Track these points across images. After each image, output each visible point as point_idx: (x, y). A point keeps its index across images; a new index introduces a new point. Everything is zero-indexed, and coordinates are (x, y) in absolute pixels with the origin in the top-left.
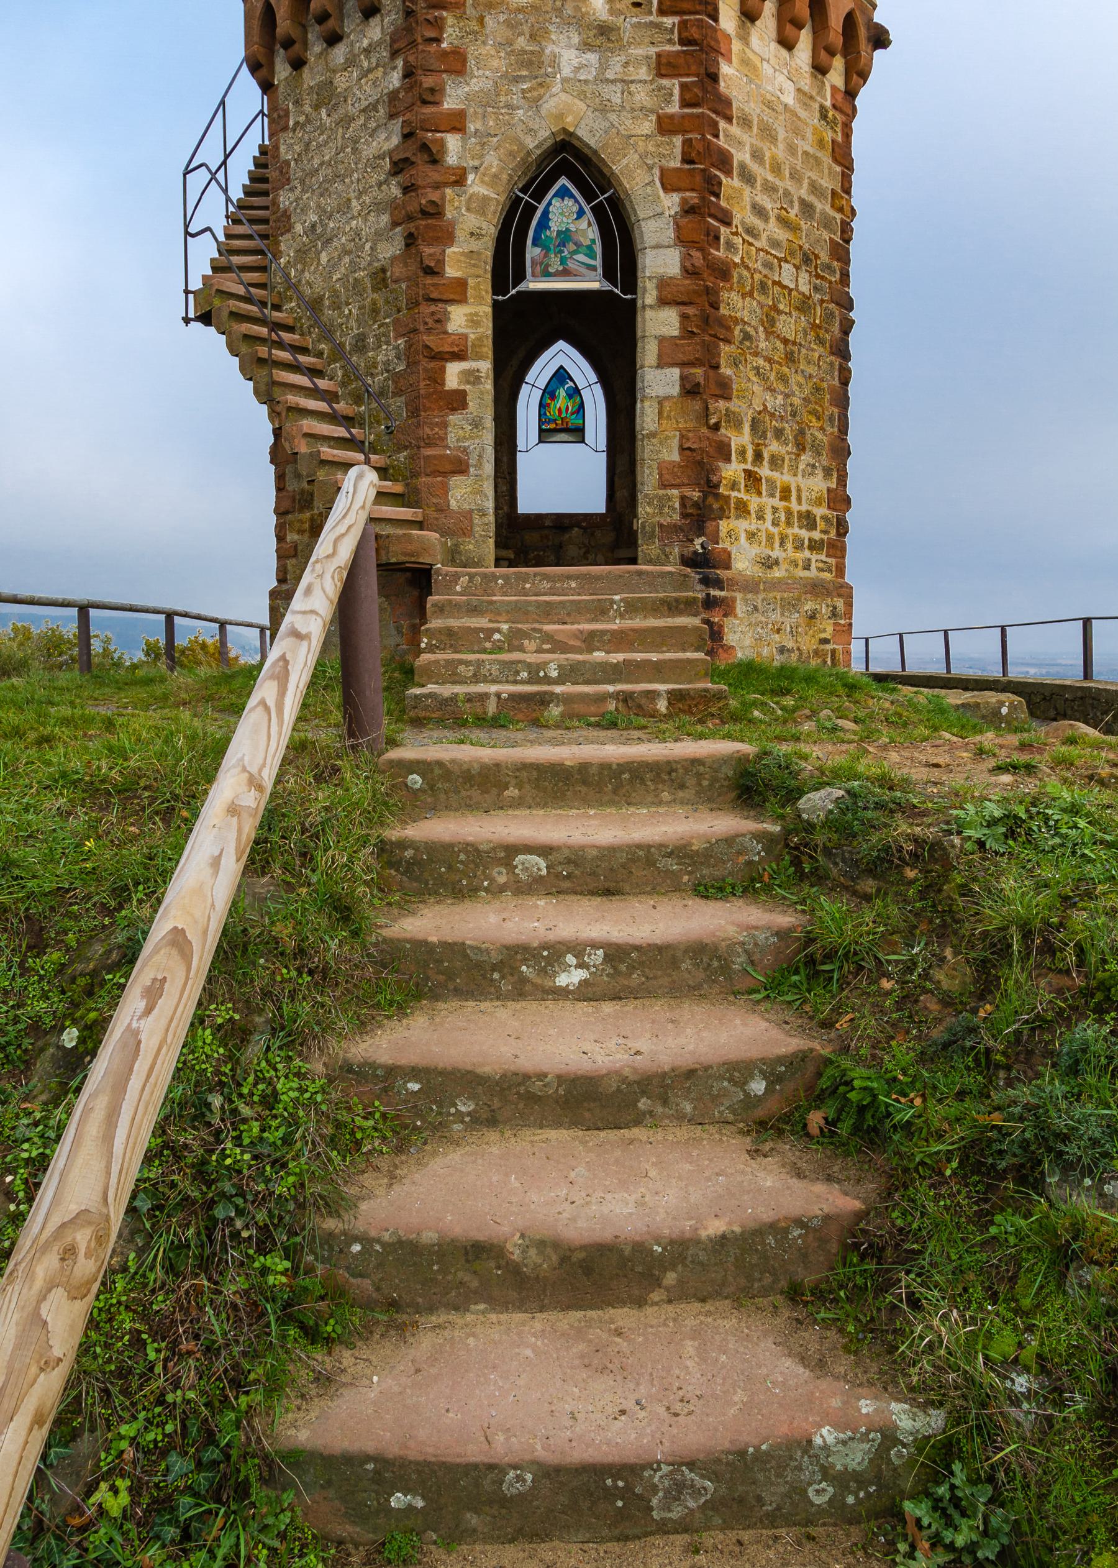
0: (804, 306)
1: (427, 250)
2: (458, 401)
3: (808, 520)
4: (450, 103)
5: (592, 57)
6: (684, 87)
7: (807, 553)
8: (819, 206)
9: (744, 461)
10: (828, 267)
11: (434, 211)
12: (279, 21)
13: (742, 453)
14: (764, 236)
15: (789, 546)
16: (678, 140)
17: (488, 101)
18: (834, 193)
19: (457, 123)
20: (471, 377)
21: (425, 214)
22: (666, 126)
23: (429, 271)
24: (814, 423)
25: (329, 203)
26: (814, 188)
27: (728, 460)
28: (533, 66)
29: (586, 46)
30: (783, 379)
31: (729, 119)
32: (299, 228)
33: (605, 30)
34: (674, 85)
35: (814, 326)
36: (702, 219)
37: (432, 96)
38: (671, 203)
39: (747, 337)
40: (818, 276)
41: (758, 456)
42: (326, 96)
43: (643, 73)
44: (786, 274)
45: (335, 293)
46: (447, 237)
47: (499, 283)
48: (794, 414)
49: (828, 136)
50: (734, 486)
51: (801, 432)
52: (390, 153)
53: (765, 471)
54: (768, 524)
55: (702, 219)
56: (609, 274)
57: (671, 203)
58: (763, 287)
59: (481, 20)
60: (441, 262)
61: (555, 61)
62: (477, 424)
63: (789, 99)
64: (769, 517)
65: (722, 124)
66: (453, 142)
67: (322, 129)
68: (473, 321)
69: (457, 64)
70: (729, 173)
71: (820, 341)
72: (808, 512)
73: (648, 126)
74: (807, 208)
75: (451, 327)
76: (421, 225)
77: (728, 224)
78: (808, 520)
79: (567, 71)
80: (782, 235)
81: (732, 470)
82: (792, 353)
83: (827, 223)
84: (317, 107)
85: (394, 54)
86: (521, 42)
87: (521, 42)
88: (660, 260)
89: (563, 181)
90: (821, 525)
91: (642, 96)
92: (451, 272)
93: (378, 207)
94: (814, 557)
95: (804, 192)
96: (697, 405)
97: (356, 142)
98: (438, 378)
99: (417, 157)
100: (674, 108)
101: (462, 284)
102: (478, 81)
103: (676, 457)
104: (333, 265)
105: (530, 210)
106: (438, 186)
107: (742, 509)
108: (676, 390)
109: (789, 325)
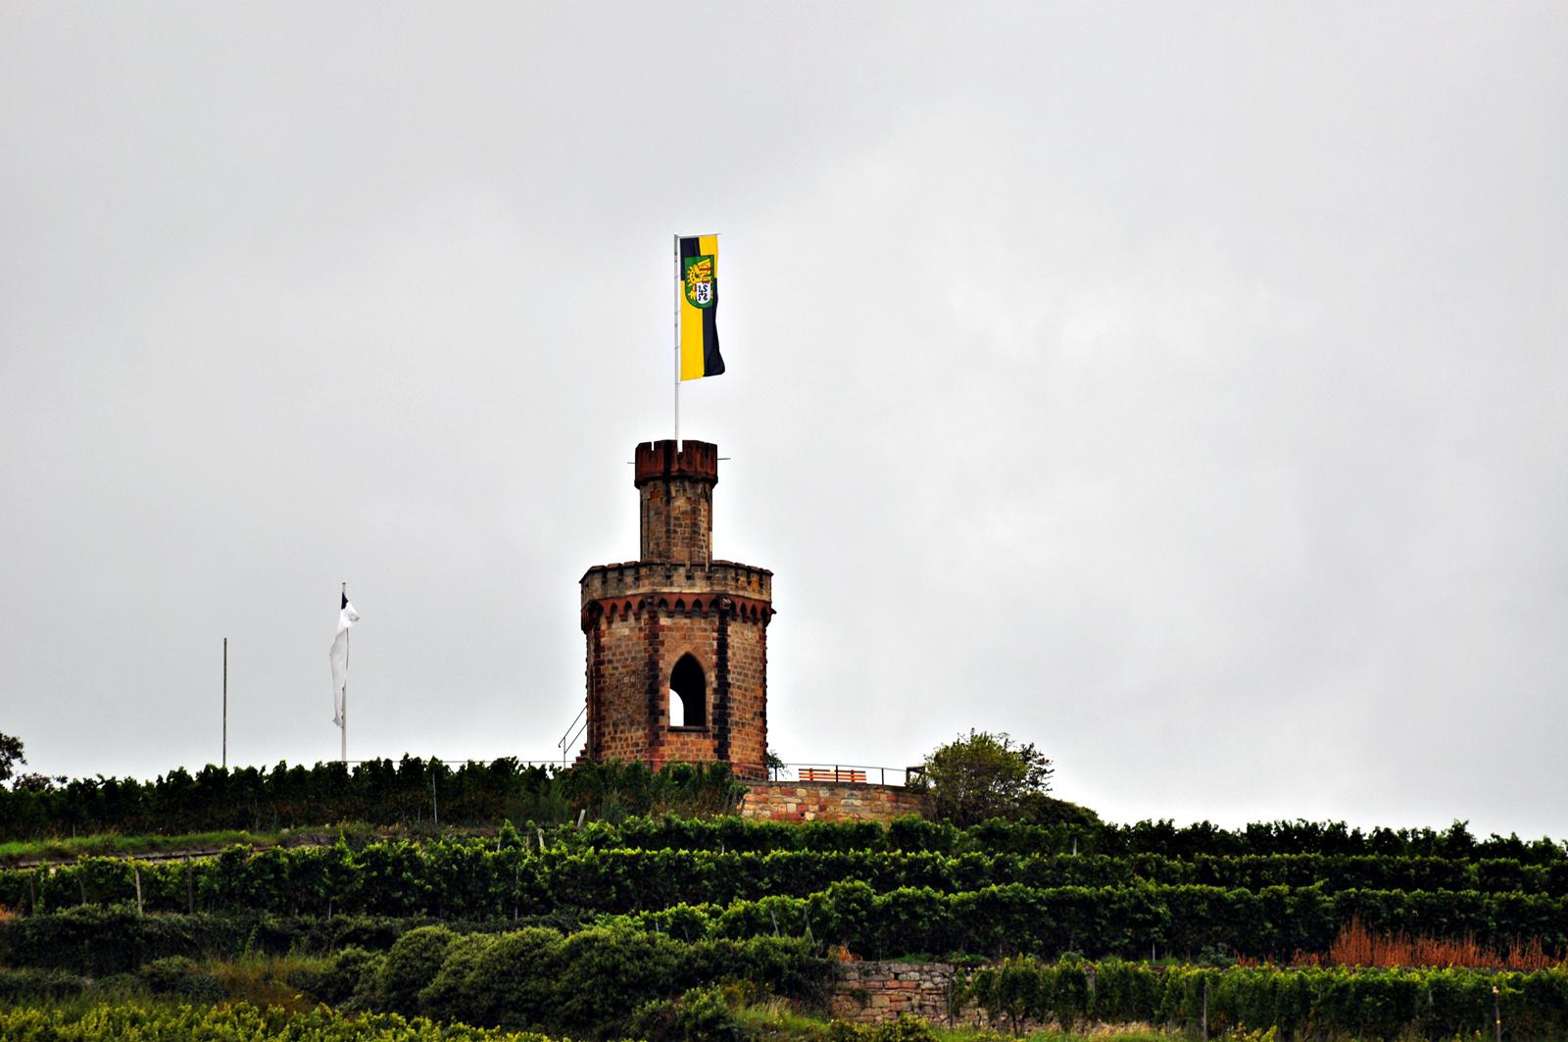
0: (633, 685)
3: (637, 745)
13: (609, 733)
24: (637, 716)
30: (625, 708)
44: (626, 680)
50: (607, 742)
54: (619, 749)
58: (617, 687)
64: (619, 747)
80: (624, 670)
81: (607, 738)
90: (641, 745)
95: (633, 655)
107: (609, 747)
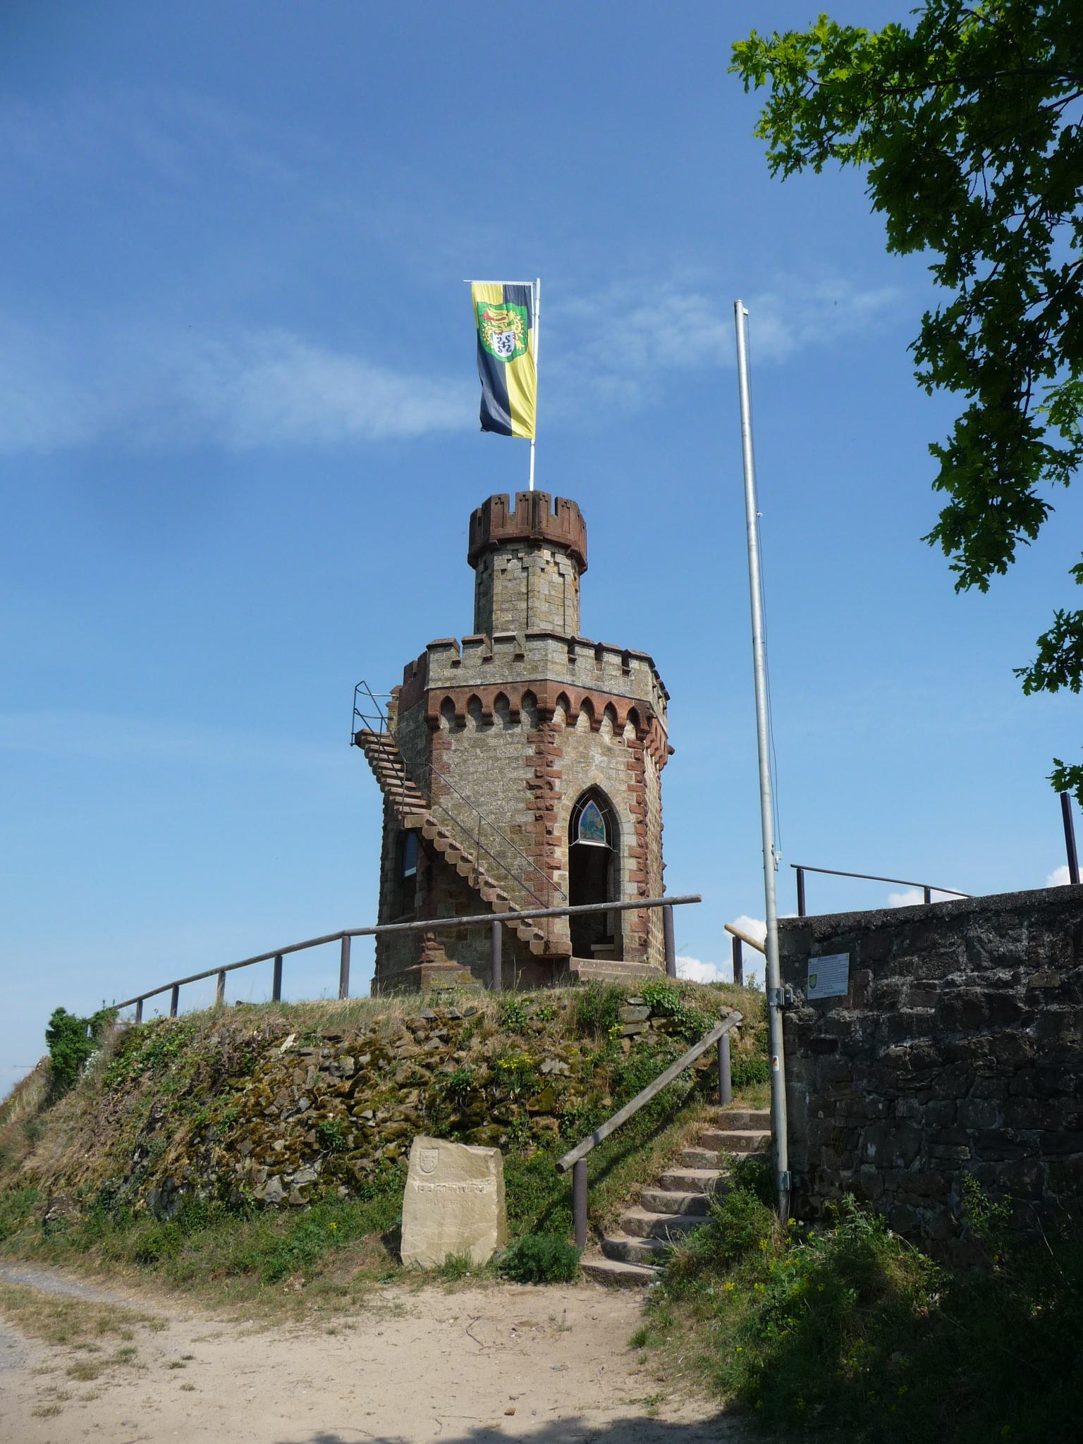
2: (556, 887)
4: (556, 767)
20: (562, 876)
21: (548, 809)
22: (631, 789)
28: (585, 759)
29: (603, 754)
33: (609, 749)
34: (633, 773)
38: (633, 817)
43: (622, 767)
46: (554, 819)
47: (570, 842)
56: (608, 842)
57: (633, 817)
61: (593, 757)
69: (559, 753)
73: (624, 787)
76: (543, 814)
85: (529, 742)
86: (581, 749)
87: (581, 749)
88: (628, 840)
91: (622, 776)
92: (556, 833)
100: (633, 782)
101: (560, 838)
105: (580, 812)
106: (552, 798)
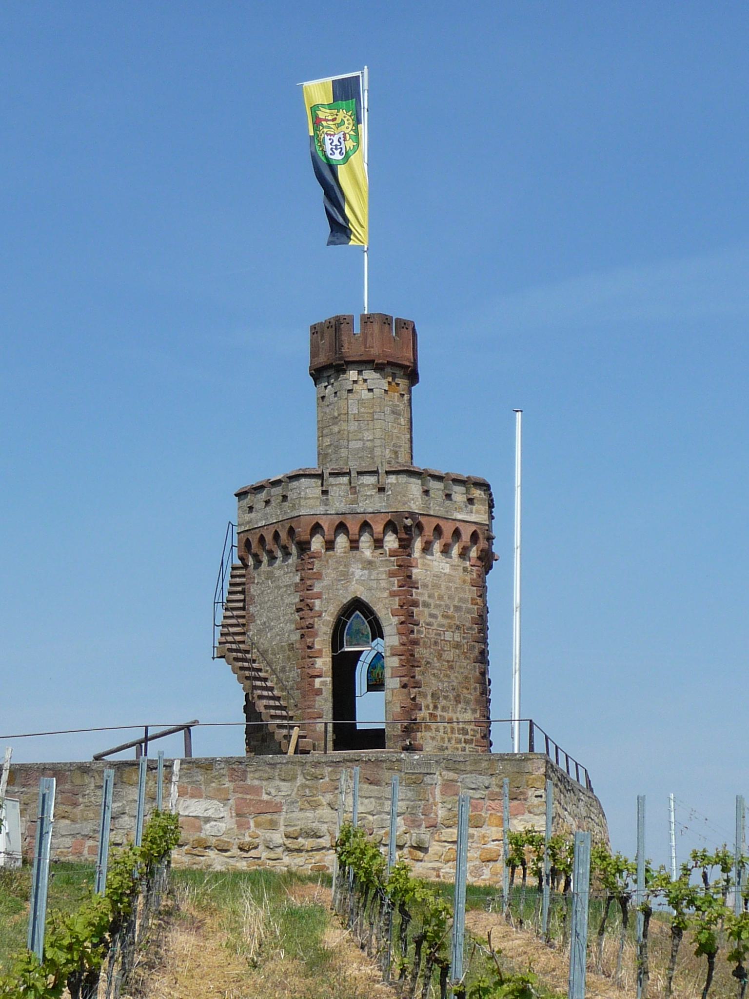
0: (457, 646)
1: (309, 640)
2: (319, 692)
4: (316, 590)
5: (366, 572)
6: (398, 580)
7: (463, 745)
8: (464, 606)
9: (429, 709)
10: (471, 628)
11: (310, 627)
12: (253, 546)
13: (427, 707)
14: (435, 624)
15: (453, 742)
16: (397, 599)
17: (329, 588)
18: (472, 599)
19: (319, 596)
20: (324, 683)
21: (308, 628)
22: (393, 594)
23: (309, 647)
24: (465, 691)
25: (271, 615)
26: (461, 600)
27: (421, 710)
28: (346, 576)
29: (363, 568)
31: (417, 588)
32: (258, 622)
33: (370, 563)
35: (464, 653)
36: (408, 621)
37: (310, 588)
38: (395, 620)
39: (428, 663)
40: (465, 633)
41: (435, 707)
42: (270, 576)
43: (384, 576)
44: (448, 636)
45: (273, 649)
46: (316, 635)
48: (453, 689)
49: (468, 578)
51: (458, 696)
52: (296, 604)
53: (439, 713)
54: (441, 733)
55: (408, 621)
58: (436, 643)
59: (327, 561)
60: (313, 644)
61: (353, 574)
62: (326, 701)
63: (447, 570)
64: (442, 731)
65: (414, 590)
66: (317, 602)
67: (269, 588)
68: (324, 663)
69: (319, 576)
70: (418, 606)
71: (466, 658)
72: (463, 728)
73: (386, 594)
74: (457, 609)
75: (317, 666)
77: (418, 625)
78: (465, 732)
79: (357, 577)
80: (445, 622)
81: (423, 714)
82: (452, 665)
83: (469, 611)
84: (267, 579)
85: (297, 571)
87: (341, 568)
89: (358, 612)
91: (383, 584)
92: (317, 647)
93: (291, 621)
94: (467, 746)
95: (456, 603)
96: (406, 690)
97: (282, 596)
98: (311, 684)
99: (304, 607)
101: (320, 651)
102: (326, 582)
103: (399, 710)
104: (273, 638)
107: (428, 728)
108: (398, 686)
109: (449, 655)
